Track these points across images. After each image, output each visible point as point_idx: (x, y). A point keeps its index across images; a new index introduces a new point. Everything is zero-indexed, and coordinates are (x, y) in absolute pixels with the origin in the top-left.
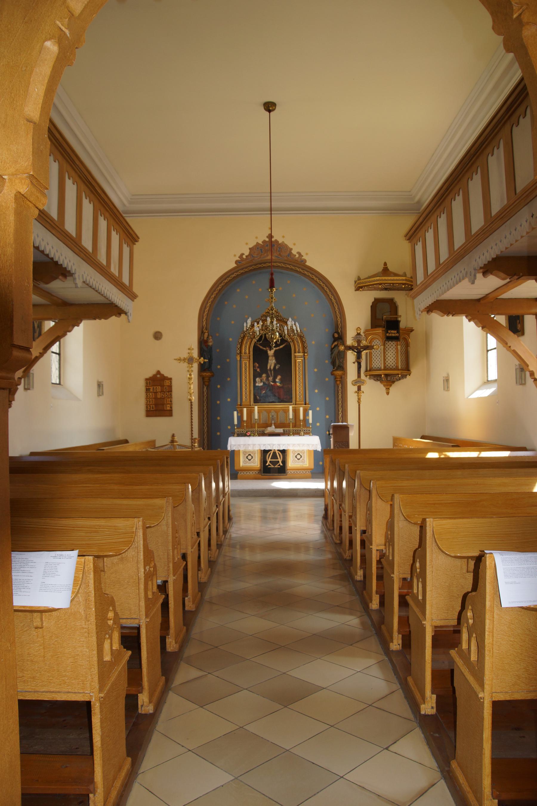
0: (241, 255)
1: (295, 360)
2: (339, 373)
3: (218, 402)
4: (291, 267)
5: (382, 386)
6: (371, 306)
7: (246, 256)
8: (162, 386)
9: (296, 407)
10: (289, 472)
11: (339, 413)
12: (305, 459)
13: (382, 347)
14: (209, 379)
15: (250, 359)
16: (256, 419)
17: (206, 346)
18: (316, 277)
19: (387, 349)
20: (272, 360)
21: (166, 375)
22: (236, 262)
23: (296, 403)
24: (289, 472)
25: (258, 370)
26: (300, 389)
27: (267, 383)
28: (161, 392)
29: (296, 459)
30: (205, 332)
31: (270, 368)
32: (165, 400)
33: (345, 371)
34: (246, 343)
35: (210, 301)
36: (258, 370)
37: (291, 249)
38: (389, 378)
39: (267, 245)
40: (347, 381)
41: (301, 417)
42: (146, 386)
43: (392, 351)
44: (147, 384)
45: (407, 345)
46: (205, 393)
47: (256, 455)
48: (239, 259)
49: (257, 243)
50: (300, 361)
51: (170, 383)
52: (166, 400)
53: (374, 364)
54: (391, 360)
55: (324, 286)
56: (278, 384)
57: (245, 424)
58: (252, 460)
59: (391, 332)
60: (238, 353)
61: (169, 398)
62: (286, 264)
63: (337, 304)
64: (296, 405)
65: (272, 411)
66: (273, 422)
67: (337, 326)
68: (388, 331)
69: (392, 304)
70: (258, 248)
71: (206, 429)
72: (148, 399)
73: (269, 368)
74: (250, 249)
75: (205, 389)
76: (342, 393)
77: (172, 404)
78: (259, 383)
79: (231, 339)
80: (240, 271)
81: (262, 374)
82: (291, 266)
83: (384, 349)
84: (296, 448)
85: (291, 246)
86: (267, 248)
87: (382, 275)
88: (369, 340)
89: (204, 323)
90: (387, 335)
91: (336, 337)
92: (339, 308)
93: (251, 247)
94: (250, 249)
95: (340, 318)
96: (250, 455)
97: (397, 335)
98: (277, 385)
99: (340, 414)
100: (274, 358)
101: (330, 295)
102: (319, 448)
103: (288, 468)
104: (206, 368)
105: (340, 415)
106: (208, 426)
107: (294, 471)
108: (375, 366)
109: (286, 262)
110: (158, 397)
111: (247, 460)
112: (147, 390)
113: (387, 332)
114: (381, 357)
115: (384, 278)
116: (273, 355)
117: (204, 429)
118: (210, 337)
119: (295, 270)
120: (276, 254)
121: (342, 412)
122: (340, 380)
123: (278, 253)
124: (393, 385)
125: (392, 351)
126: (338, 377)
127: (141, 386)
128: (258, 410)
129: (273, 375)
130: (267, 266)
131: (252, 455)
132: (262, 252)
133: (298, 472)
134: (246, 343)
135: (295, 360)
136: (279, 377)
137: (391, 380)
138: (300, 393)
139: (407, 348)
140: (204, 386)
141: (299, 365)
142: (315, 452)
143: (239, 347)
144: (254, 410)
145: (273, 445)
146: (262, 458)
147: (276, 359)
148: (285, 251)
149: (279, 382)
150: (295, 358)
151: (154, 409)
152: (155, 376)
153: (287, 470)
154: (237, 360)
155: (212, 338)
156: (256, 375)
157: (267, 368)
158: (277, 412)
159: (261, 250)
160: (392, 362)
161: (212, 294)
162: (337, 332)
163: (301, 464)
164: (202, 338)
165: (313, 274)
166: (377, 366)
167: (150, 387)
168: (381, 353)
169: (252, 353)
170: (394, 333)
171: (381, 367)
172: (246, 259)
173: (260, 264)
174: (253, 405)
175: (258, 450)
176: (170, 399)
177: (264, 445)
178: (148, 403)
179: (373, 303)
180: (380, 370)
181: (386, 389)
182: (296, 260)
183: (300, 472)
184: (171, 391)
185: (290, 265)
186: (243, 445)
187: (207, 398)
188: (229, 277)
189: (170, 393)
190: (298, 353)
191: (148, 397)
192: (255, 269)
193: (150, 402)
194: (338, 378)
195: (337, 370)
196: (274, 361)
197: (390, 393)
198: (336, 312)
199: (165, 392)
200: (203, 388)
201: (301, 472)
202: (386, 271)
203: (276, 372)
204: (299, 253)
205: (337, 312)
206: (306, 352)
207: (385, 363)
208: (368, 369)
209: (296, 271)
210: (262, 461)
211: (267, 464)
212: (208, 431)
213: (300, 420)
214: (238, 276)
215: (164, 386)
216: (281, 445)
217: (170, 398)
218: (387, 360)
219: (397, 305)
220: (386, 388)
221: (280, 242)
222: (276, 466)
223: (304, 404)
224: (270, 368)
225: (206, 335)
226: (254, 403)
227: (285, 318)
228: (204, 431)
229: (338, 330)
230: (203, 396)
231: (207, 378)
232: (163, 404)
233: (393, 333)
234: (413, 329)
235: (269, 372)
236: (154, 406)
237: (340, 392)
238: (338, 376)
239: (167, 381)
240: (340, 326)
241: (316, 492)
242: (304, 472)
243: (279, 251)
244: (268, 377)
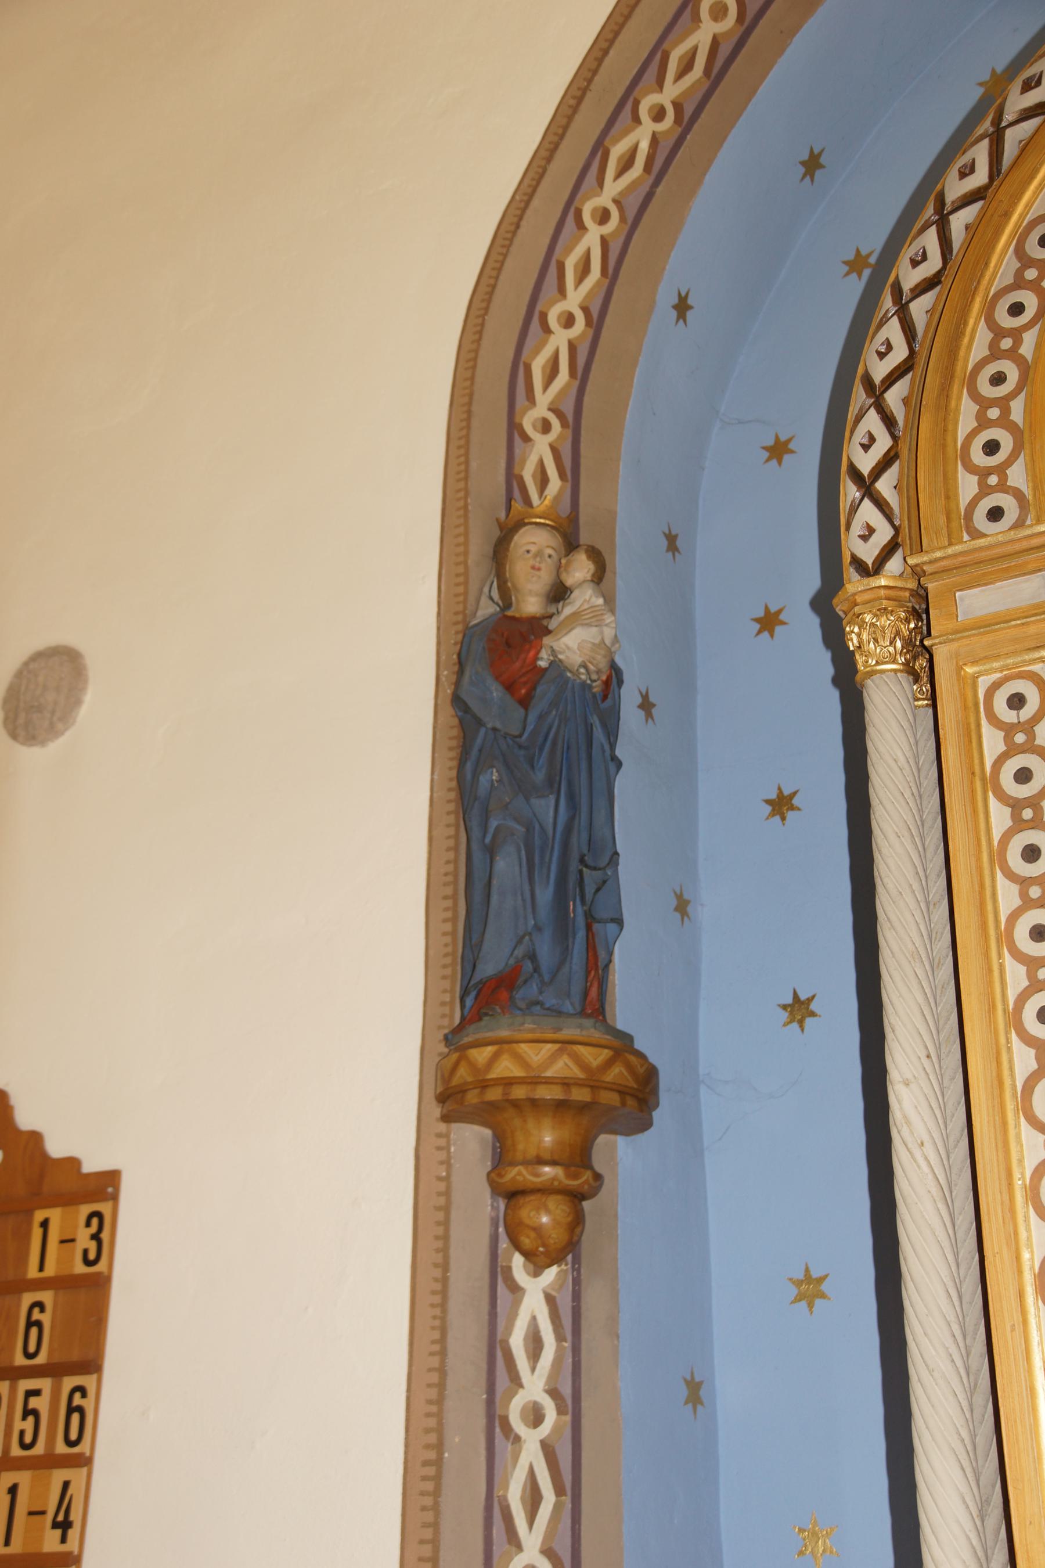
35: (605, 199)
51: (84, 1240)
60: (868, 553)
143: (866, 463)
176: (59, 1476)
184: (92, 1365)
189: (69, 1383)
239: (55, 1215)
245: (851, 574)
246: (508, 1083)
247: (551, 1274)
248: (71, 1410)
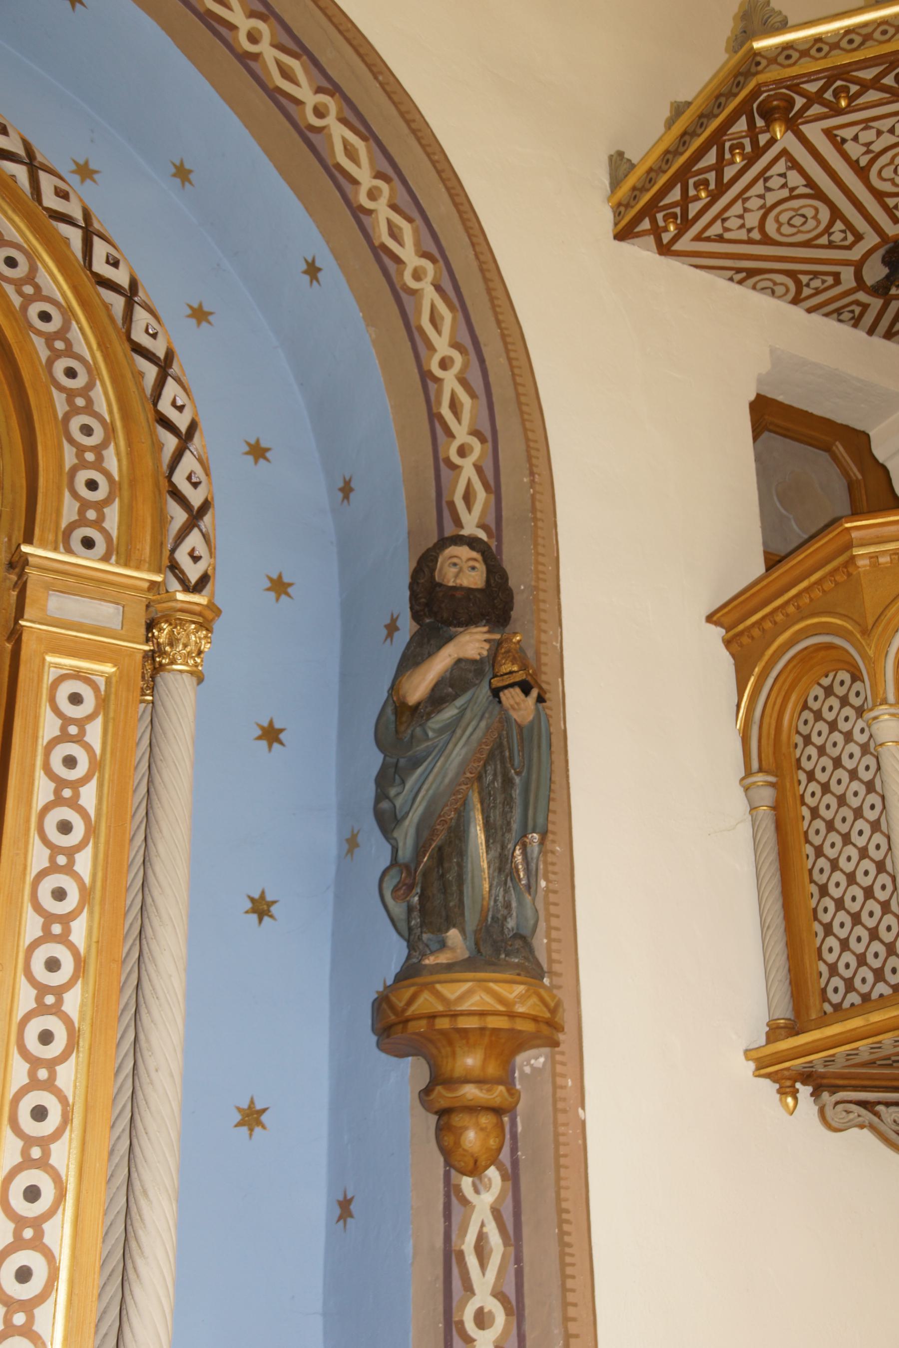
91: (470, 590)
122: (497, 1111)
205: (450, 381)
206: (193, 573)
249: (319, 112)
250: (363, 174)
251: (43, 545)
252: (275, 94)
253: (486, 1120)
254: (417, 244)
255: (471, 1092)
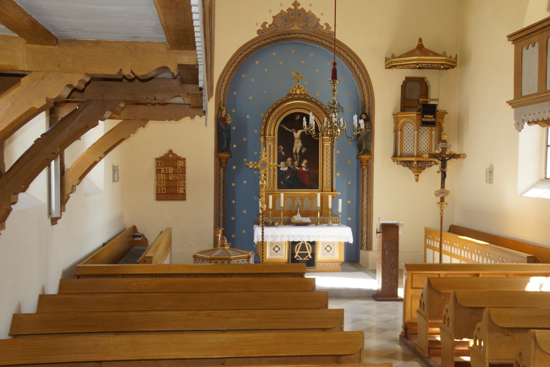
0: (263, 24)
1: (323, 143)
2: (365, 157)
3: (233, 184)
4: (317, 39)
5: (411, 172)
6: (402, 86)
7: (269, 26)
8: (175, 167)
9: (322, 194)
10: (318, 265)
11: (364, 199)
12: (335, 251)
13: (416, 132)
14: (227, 161)
15: (274, 141)
16: (281, 207)
17: (224, 124)
18: (344, 52)
19: (420, 134)
20: (298, 143)
21: (179, 155)
22: (259, 31)
23: (322, 190)
24: (318, 265)
25: (283, 153)
26: (327, 174)
27: (292, 167)
28: (173, 174)
29: (326, 251)
30: (223, 109)
31: (296, 151)
32: (178, 183)
33: (371, 155)
34: (271, 123)
35: (228, 74)
36: (283, 153)
37: (319, 20)
38: (420, 165)
39: (293, 14)
40: (373, 166)
41: (330, 206)
42: (156, 167)
43: (426, 136)
44: (158, 164)
45: (441, 130)
46: (222, 176)
47: (284, 246)
48: (261, 28)
49: (282, 11)
50: (328, 145)
51: (183, 163)
52: (179, 182)
53: (405, 150)
54: (424, 146)
55: (352, 62)
56: (304, 169)
57: (270, 213)
58: (279, 252)
59: (427, 116)
60: (262, 134)
61: (182, 180)
62: (312, 36)
63: (366, 83)
64: (322, 192)
65: (297, 197)
66: (298, 210)
67: (364, 106)
68: (424, 116)
69: (423, 84)
70: (282, 17)
71: (222, 214)
72: (159, 181)
73: (294, 151)
74: (273, 17)
75: (222, 171)
76: (367, 179)
77: (185, 187)
78: (284, 168)
79: (248, 117)
80: (262, 42)
81: (287, 158)
82: (317, 38)
83: (418, 134)
84: (327, 240)
85: (318, 16)
86: (292, 17)
87: (420, 54)
88: (402, 124)
89: (222, 99)
90: (423, 119)
92: (367, 87)
93: (275, 15)
94: (273, 17)
95: (369, 98)
96: (277, 246)
97: (433, 120)
98: (302, 169)
99: (365, 200)
100: (300, 141)
101: (358, 72)
102: (351, 241)
103: (317, 260)
104: (224, 148)
105: (365, 202)
106: (223, 211)
107: (323, 264)
108: (406, 152)
109: (313, 34)
110: (170, 179)
111: (274, 252)
112: (158, 171)
113: (423, 117)
114: (414, 142)
115: (422, 58)
116: (299, 137)
117: (220, 214)
118: (229, 115)
119: (321, 43)
120: (302, 25)
121: (367, 198)
122: (366, 165)
123: (304, 23)
124: (423, 171)
125: (426, 136)
126: (364, 161)
127: (150, 167)
128: (284, 197)
129: (298, 159)
130: (291, 37)
131: (279, 246)
132: (287, 22)
133: (327, 265)
134: (271, 123)
135: (323, 143)
136: (305, 161)
137: (422, 167)
138: (327, 179)
139: (441, 133)
140: (221, 168)
141: (327, 149)
142: (347, 244)
143: (263, 128)
144: (280, 197)
145: (303, 236)
146: (290, 250)
147: (303, 142)
148: (312, 21)
149: (305, 167)
150: (323, 141)
151: (165, 192)
152: (166, 155)
153: (316, 262)
154: (261, 142)
155: (230, 116)
156: (281, 159)
157: (293, 151)
158: (302, 199)
159: (286, 19)
160: (426, 148)
161: (231, 66)
162: (365, 114)
163: (331, 256)
164: (220, 115)
165: (341, 49)
166: (408, 152)
167: (161, 168)
168: (414, 138)
169: (276, 134)
170: (430, 118)
171: (413, 153)
172: (269, 28)
173: (285, 35)
174: (276, 191)
175: (286, 242)
176: (183, 181)
177: (293, 236)
178: (159, 186)
179: (404, 82)
180: (412, 156)
181: (415, 176)
182: (324, 33)
183: (329, 265)
184: (185, 173)
185: (316, 37)
186: (270, 236)
187: (223, 180)
188: (249, 48)
189: (183, 175)
190: (326, 136)
191: (159, 179)
192: (278, 40)
193: (161, 184)
194: (364, 163)
195: (363, 154)
196: (300, 144)
197: (419, 180)
198: (363, 91)
199: (178, 174)
200: (220, 169)
201: (331, 265)
202: (421, 49)
203: (302, 156)
204: (327, 25)
205: (365, 91)
207: (418, 149)
208: (399, 154)
209: (322, 44)
210: (290, 253)
211: (296, 257)
212: (223, 217)
213: (329, 209)
214: (259, 47)
215: (177, 167)
216: (311, 237)
217: (184, 180)
218: (420, 146)
219: (428, 85)
220: (415, 174)
221: (307, 11)
222: (305, 259)
223: (331, 191)
224: (296, 151)
225: (224, 112)
226: (278, 189)
227: (313, 98)
228: (220, 217)
229: (365, 110)
230: (220, 179)
231: (225, 160)
232: (176, 187)
233: (429, 118)
234: (447, 112)
235: (295, 156)
236: (165, 189)
237: (365, 177)
238: (365, 160)
239: (180, 162)
240: (367, 107)
241: (360, 293)
242: (334, 265)
243: (305, 22)
244: (293, 161)
245: (261, 135)
246: (225, 157)
247: (223, 168)
248: (184, 176)
249: (351, 61)
250: (356, 68)
251: (324, 137)
252: (346, 60)
253: (365, 166)
254: (362, 76)
255: (363, 164)
